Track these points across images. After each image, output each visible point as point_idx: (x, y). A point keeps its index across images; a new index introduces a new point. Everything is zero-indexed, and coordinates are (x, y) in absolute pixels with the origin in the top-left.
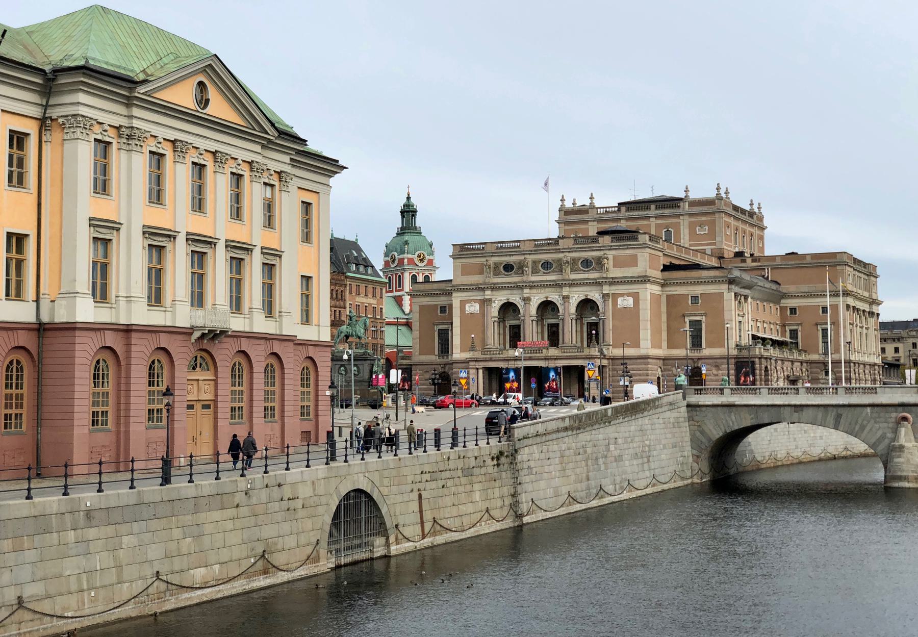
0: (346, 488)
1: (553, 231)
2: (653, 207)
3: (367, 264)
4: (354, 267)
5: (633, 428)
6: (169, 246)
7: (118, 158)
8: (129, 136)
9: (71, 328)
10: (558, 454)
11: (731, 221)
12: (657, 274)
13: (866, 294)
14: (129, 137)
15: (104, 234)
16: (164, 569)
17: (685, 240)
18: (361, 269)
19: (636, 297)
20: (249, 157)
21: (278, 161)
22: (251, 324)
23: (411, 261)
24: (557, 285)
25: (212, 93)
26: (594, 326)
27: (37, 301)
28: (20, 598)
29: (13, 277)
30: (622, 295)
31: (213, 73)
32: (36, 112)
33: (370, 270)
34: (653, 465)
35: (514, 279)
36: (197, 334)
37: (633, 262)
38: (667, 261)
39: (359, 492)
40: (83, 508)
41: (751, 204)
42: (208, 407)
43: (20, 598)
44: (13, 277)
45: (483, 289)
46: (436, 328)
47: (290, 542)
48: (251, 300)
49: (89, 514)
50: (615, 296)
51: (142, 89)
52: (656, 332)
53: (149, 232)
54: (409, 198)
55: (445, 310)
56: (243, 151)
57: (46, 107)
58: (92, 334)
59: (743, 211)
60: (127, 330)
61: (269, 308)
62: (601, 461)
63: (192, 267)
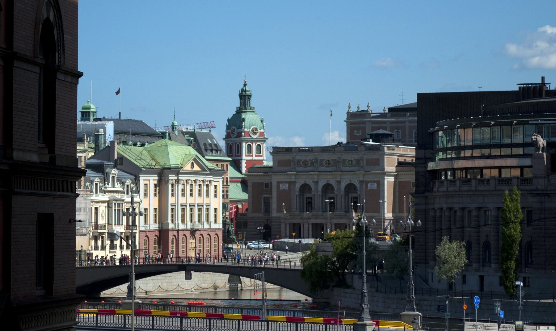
3: (218, 150)
23: (248, 134)
25: (195, 164)
30: (371, 182)
38: (402, 159)
50: (367, 183)
54: (245, 85)
55: (268, 186)
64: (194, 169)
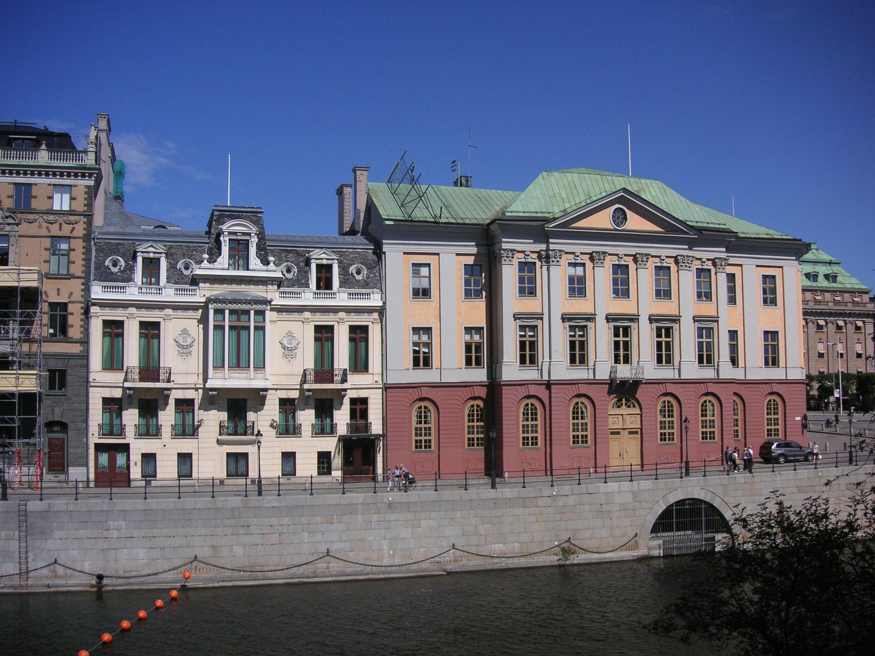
0: (673, 499)
7: (541, 272)
16: (459, 544)
40: (385, 500)
42: (636, 433)
47: (604, 533)
49: (390, 505)
56: (667, 251)
60: (549, 385)
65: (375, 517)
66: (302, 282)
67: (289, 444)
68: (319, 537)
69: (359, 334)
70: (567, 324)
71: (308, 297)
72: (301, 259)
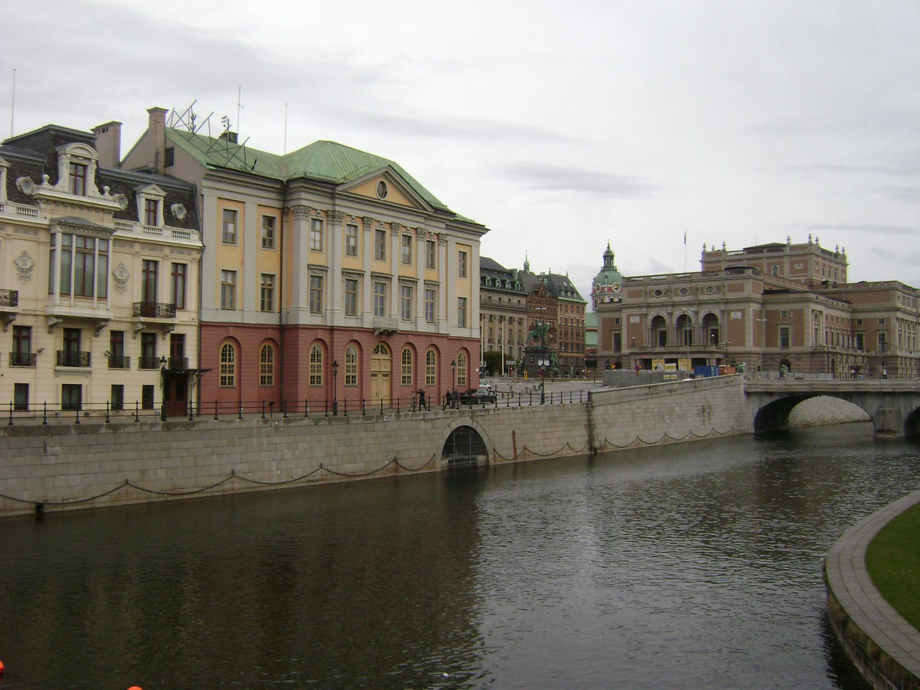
0: (454, 426)
1: (698, 268)
2: (765, 251)
3: (573, 291)
4: (563, 293)
5: (696, 397)
6: (360, 280)
8: (333, 216)
9: (296, 328)
10: (629, 411)
11: (820, 260)
12: (758, 296)
13: (914, 310)
14: (333, 217)
15: (318, 275)
16: (326, 463)
17: (787, 273)
18: (569, 294)
19: (743, 311)
20: (415, 225)
21: (437, 228)
22: (416, 327)
23: (610, 289)
24: (690, 304)
25: (389, 188)
26: (715, 332)
27: (280, 312)
28: (233, 471)
29: (266, 299)
30: (733, 311)
31: (391, 176)
32: (277, 204)
33: (575, 295)
34: (712, 421)
35: (662, 299)
36: (377, 332)
37: (741, 288)
39: (466, 428)
41: (837, 248)
42: (387, 375)
43: (233, 471)
44: (266, 299)
45: (642, 307)
46: (613, 333)
48: (416, 312)
50: (729, 312)
51: (340, 188)
52: (757, 335)
53: (345, 272)
56: (410, 222)
57: (284, 201)
58: (309, 331)
59: (830, 253)
60: (332, 329)
61: (431, 316)
62: (667, 417)
63: (376, 292)
64: (387, 198)
65: (266, 441)
66: (131, 213)
67: (118, 376)
68: (225, 459)
69: (179, 271)
70: (345, 278)
71: (137, 231)
72: (130, 192)
